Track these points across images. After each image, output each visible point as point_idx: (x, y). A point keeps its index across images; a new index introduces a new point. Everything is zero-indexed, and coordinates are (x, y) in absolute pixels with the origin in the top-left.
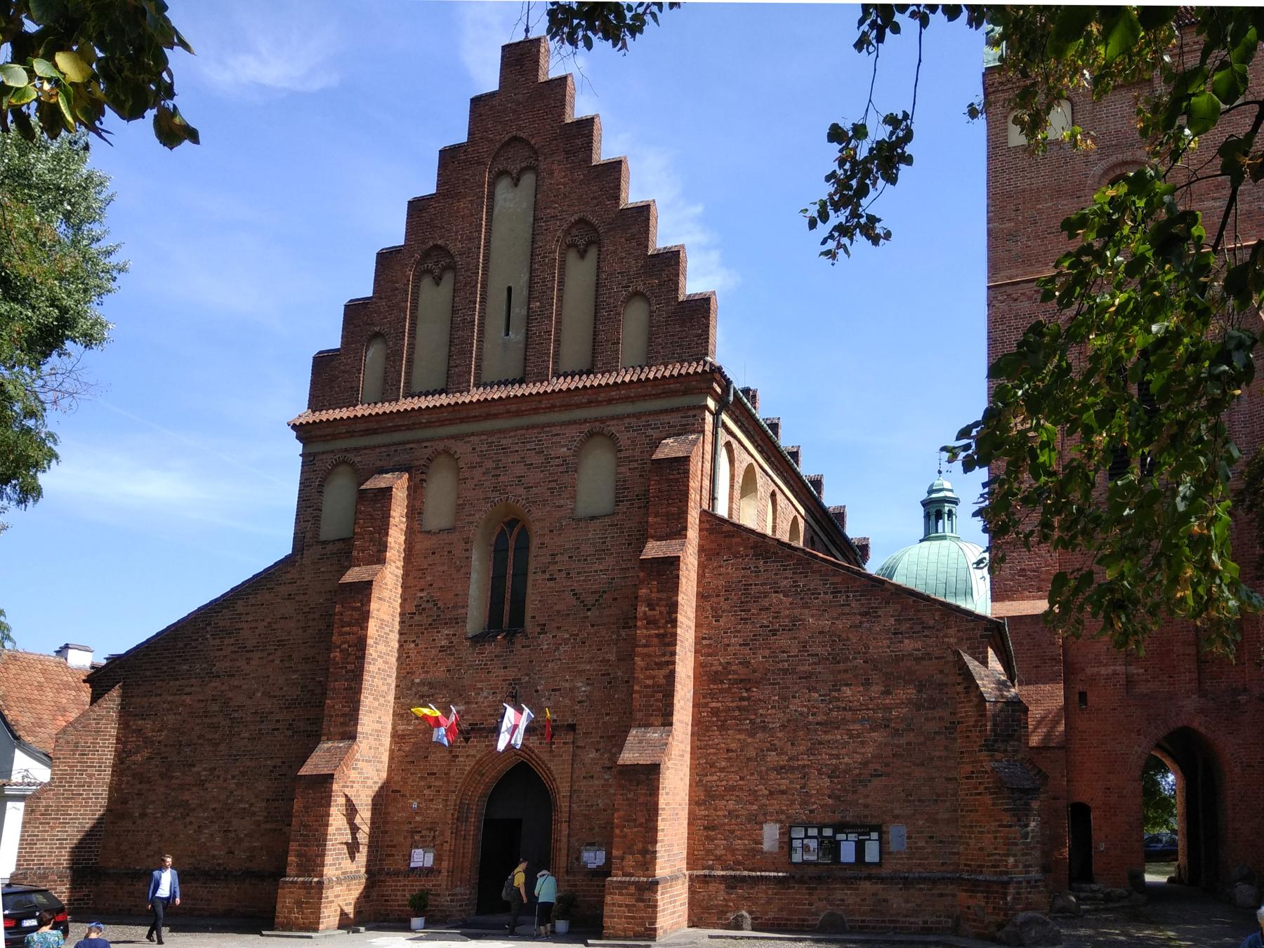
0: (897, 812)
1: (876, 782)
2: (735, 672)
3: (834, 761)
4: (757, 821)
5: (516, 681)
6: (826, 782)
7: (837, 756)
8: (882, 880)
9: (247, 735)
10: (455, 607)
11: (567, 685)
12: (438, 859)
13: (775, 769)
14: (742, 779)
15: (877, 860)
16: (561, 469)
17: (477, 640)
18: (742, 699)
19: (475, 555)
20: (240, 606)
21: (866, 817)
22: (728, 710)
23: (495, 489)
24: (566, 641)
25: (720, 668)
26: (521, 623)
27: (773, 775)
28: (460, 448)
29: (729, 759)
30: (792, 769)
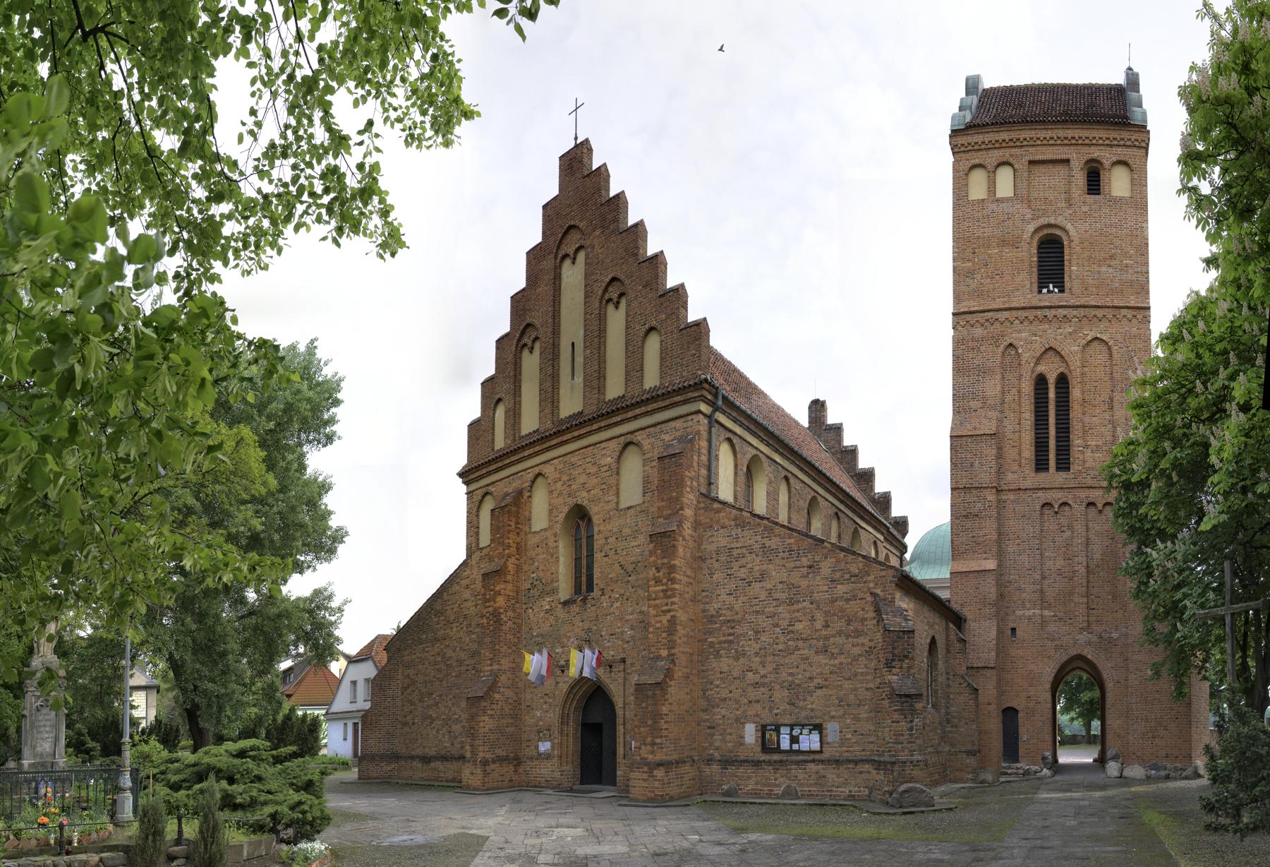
1: (819, 692)
4: (740, 721)
5: (589, 630)
6: (786, 693)
8: (822, 762)
10: (552, 581)
12: (553, 747)
17: (565, 603)
18: (730, 635)
19: (561, 544)
22: (720, 643)
23: (570, 495)
24: (617, 599)
26: (590, 588)
27: (750, 689)
28: (547, 469)
29: (722, 679)
30: (764, 685)
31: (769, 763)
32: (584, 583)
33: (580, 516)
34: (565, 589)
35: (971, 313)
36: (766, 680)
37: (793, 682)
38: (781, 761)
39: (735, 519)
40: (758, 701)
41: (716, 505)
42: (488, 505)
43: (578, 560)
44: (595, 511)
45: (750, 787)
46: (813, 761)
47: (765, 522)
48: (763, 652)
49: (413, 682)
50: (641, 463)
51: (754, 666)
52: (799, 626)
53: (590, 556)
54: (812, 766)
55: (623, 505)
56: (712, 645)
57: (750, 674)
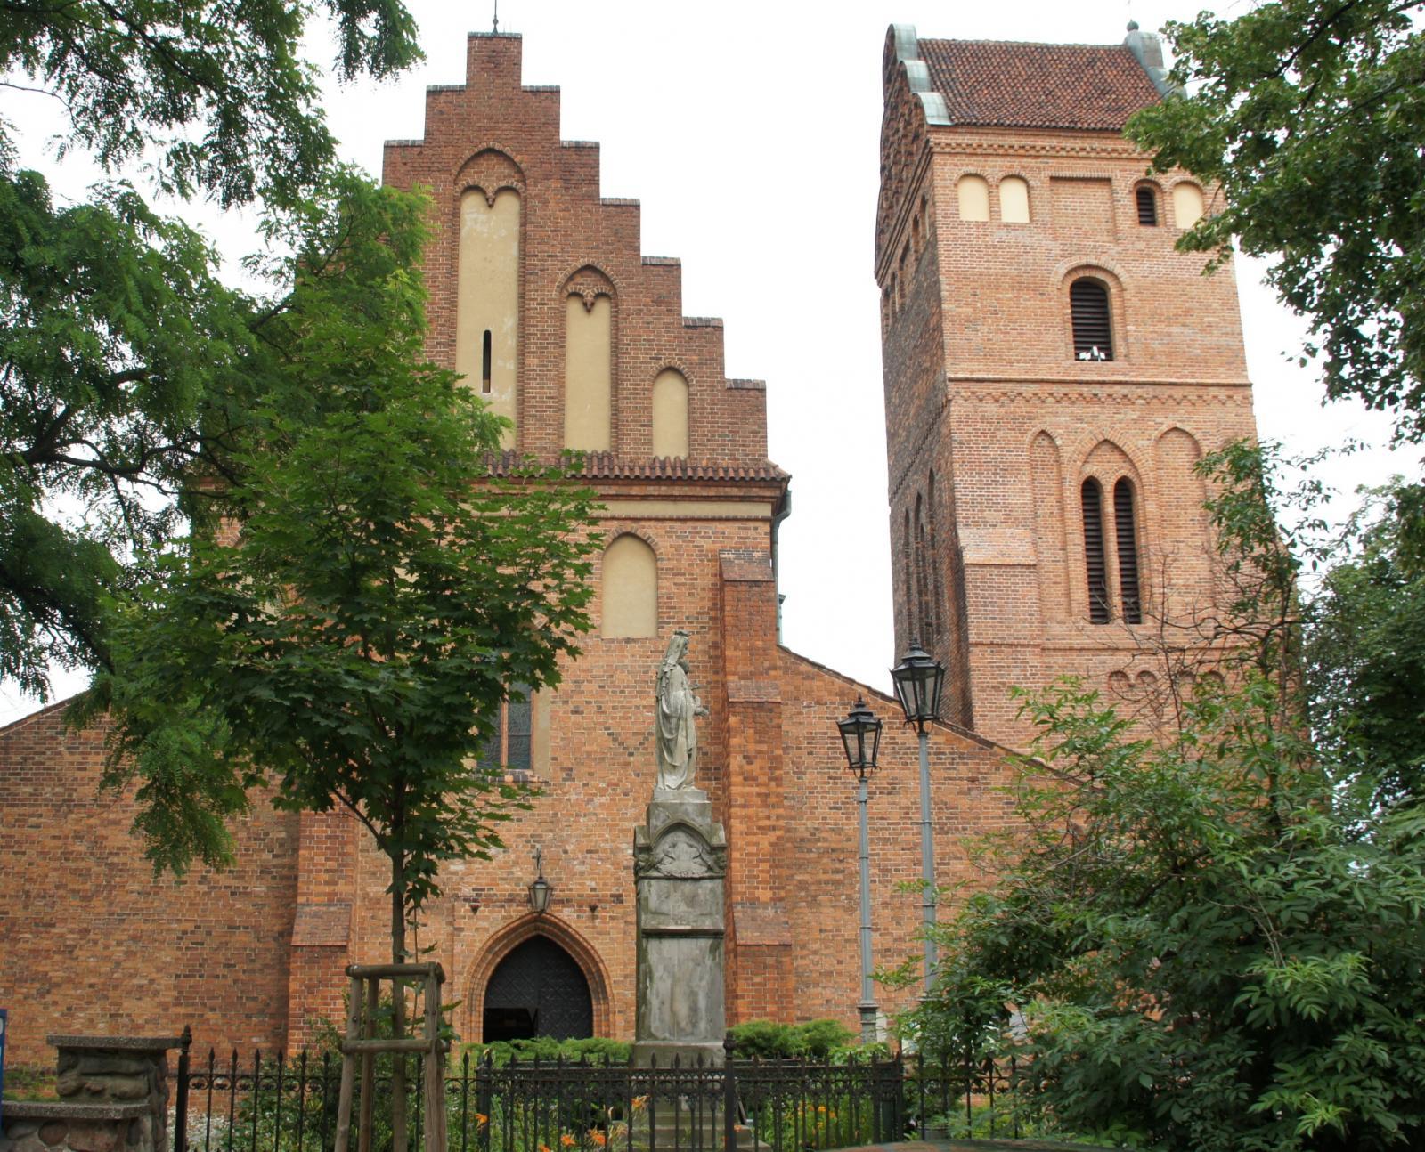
2: (826, 840)
13: (879, 952)
14: (840, 962)
18: (837, 871)
22: (819, 883)
25: (807, 835)
29: (823, 941)
30: (900, 952)
36: (904, 946)
48: (897, 902)
51: (881, 923)
56: (802, 886)
57: (876, 936)
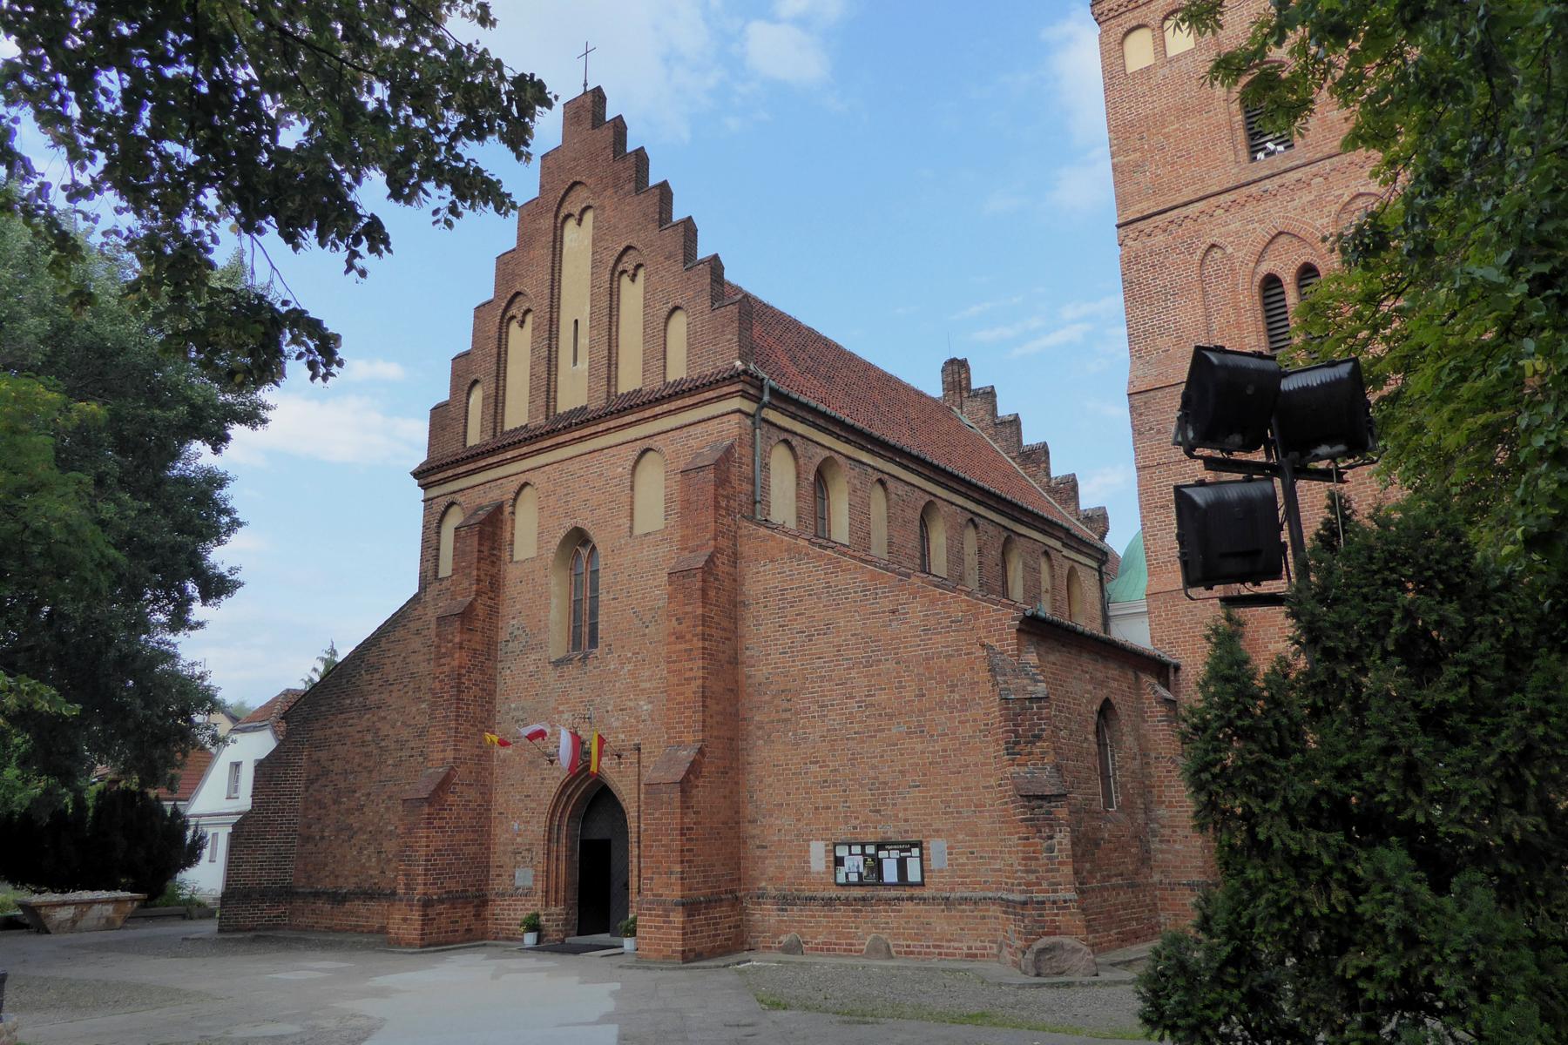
0: (937, 825)
1: (916, 793)
3: (872, 773)
4: (805, 839)
7: (874, 767)
9: (390, 762)
11: (631, 704)
15: (918, 879)
16: (617, 489)
17: (558, 663)
20: (384, 644)
21: (906, 832)
24: (629, 660)
26: (594, 642)
31: (847, 902)
32: (585, 633)
33: (578, 539)
34: (557, 643)
35: (1144, 218)
37: (876, 778)
38: (864, 899)
39: (788, 550)
40: (828, 808)
41: (763, 531)
42: (454, 519)
43: (577, 602)
44: (597, 537)
45: (820, 939)
46: (911, 899)
47: (828, 552)
49: (326, 772)
50: (663, 476)
52: (881, 697)
53: (595, 598)
54: (909, 906)
55: (638, 531)
57: (814, 768)
